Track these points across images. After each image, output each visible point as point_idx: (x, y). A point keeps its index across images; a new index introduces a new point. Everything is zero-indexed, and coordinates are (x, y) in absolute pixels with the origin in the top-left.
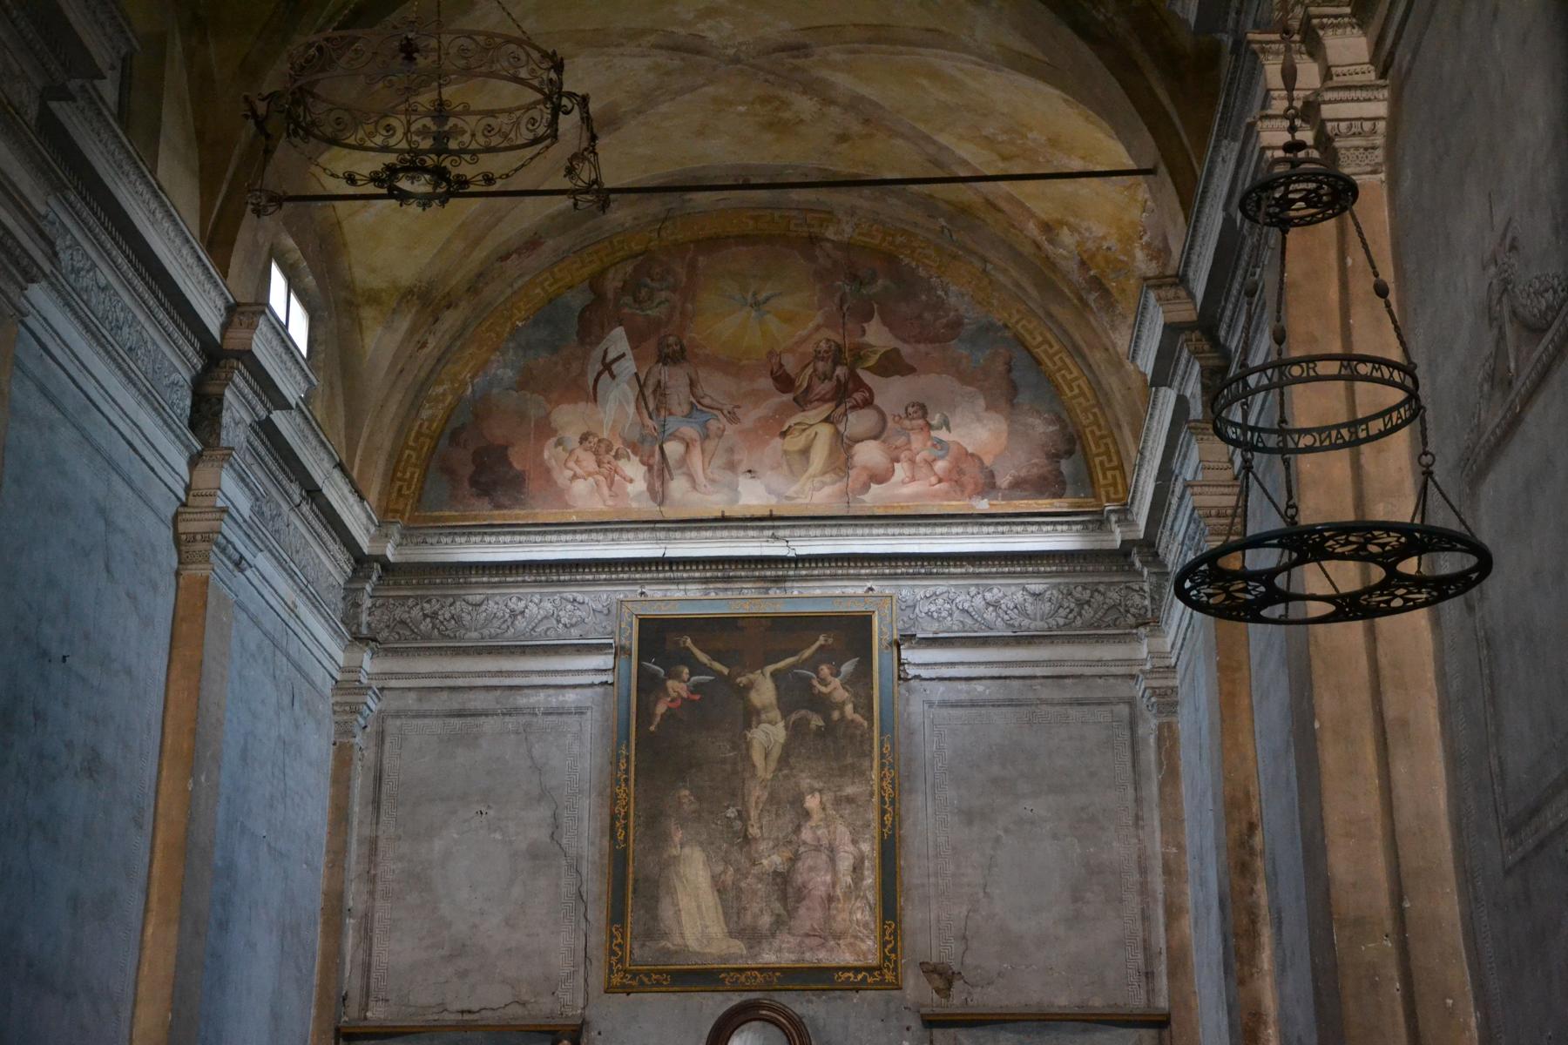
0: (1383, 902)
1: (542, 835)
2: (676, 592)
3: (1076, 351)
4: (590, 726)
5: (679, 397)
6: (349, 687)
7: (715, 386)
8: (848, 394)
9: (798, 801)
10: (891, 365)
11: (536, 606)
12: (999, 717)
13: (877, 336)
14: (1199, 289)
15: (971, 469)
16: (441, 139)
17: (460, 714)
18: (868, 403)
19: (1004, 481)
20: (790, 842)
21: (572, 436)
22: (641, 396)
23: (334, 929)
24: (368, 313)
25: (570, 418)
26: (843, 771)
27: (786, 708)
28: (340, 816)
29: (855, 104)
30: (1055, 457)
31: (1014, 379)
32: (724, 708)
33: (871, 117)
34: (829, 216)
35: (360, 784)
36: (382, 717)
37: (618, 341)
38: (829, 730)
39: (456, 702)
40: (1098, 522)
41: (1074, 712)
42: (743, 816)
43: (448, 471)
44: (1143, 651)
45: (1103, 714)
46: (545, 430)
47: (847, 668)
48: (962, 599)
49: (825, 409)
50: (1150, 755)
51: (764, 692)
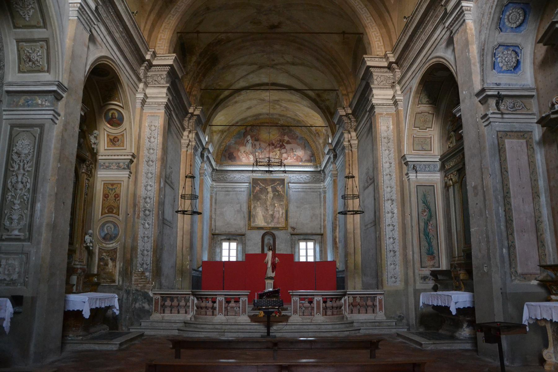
0: (352, 230)
1: (239, 208)
2: (257, 175)
3: (314, 141)
4: (245, 193)
5: (258, 146)
6: (212, 187)
7: (263, 145)
8: (282, 146)
9: (274, 204)
10: (288, 143)
11: (238, 176)
12: (302, 194)
13: (286, 138)
14: (334, 146)
15: (299, 158)
16: (269, 162)
17: (227, 191)
18: (285, 148)
19: (304, 160)
20: (273, 210)
21: (242, 151)
22: (252, 146)
23: (211, 220)
24: (214, 134)
25: (242, 149)
26: (280, 201)
27: (273, 192)
28: (211, 205)
29: (285, 107)
30: (311, 157)
31: (305, 145)
32: (264, 190)
33: (287, 109)
34: (279, 120)
35: (213, 200)
36: (216, 191)
37: (249, 137)
38: (279, 194)
39: (227, 189)
40: (317, 167)
41: (312, 193)
42: (267, 207)
43: (225, 156)
44: (322, 185)
45: (316, 193)
46: (239, 150)
47: (281, 186)
48: (297, 177)
49: (279, 149)
50: (322, 199)
51: (270, 189)
